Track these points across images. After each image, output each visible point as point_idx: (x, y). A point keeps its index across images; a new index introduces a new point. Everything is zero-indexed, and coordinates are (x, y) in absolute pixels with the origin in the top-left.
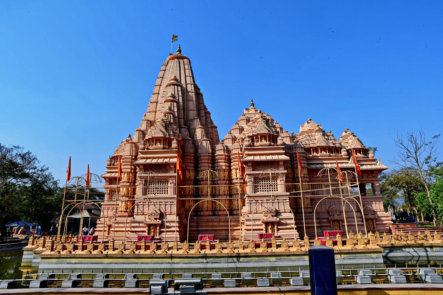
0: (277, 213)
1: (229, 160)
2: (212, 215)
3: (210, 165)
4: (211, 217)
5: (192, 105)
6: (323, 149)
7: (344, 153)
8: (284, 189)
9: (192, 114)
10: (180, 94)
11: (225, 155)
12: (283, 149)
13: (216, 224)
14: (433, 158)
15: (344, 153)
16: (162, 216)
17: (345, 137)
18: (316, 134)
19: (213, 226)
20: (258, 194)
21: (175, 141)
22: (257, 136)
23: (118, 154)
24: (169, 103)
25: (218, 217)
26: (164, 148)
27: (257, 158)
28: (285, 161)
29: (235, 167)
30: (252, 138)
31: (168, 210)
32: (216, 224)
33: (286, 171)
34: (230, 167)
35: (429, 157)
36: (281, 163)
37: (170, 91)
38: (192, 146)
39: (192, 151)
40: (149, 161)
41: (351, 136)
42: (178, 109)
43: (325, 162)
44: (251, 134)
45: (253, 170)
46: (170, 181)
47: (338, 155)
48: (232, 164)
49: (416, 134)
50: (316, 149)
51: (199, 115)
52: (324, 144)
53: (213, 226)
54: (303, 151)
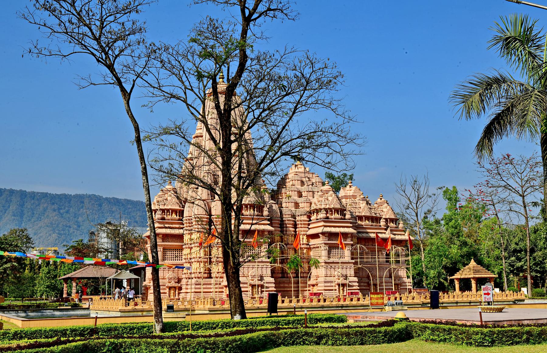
0: (346, 277)
1: (295, 226)
2: (282, 277)
3: (279, 229)
4: (281, 279)
6: (367, 218)
7: (382, 223)
8: (350, 258)
11: (293, 221)
12: (351, 223)
13: (286, 285)
14: (433, 213)
15: (382, 223)
16: (261, 278)
17: (381, 204)
18: (361, 202)
19: (284, 287)
20: (331, 260)
23: (166, 207)
25: (288, 279)
27: (333, 230)
31: (264, 273)
32: (286, 285)
33: (352, 242)
35: (430, 211)
36: (349, 236)
41: (386, 205)
43: (368, 231)
46: (264, 246)
47: (377, 224)
48: (297, 230)
49: (421, 180)
50: (361, 218)
52: (368, 214)
53: (284, 287)
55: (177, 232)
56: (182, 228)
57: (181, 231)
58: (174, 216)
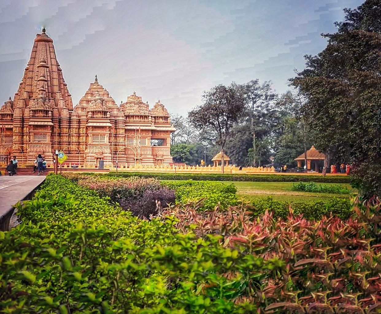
5: (56, 82)
9: (56, 89)
10: (48, 75)
21: (50, 112)
22: (96, 111)
24: (42, 82)
26: (44, 116)
28: (109, 127)
29: (82, 126)
30: (93, 112)
34: (79, 126)
37: (42, 71)
38: (58, 113)
39: (58, 115)
40: (36, 123)
42: (48, 86)
44: (92, 110)
45: (92, 131)
51: (60, 89)
54: (123, 119)
55: (9, 126)
56: (12, 125)
57: (12, 126)
58: (9, 118)
